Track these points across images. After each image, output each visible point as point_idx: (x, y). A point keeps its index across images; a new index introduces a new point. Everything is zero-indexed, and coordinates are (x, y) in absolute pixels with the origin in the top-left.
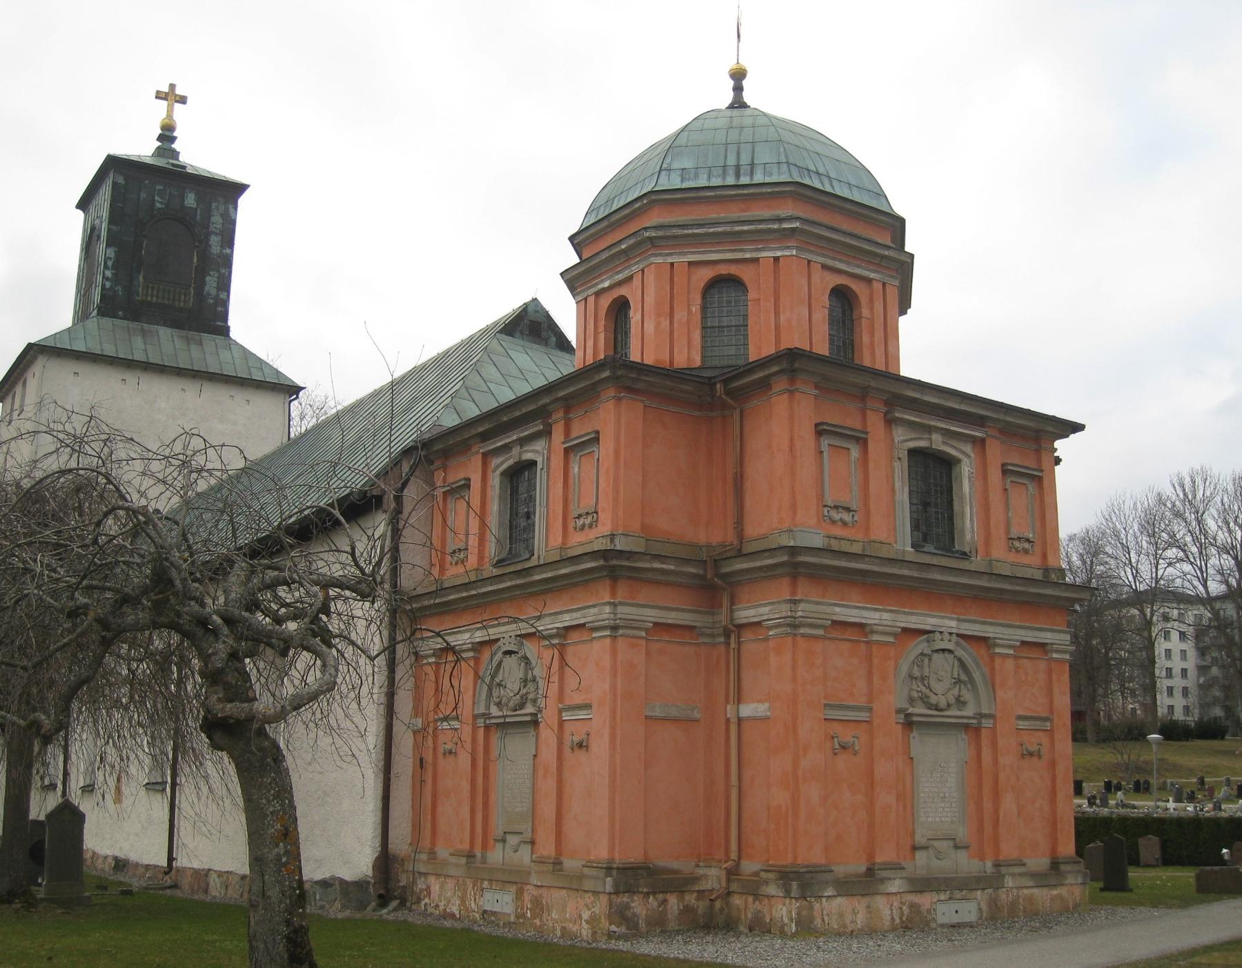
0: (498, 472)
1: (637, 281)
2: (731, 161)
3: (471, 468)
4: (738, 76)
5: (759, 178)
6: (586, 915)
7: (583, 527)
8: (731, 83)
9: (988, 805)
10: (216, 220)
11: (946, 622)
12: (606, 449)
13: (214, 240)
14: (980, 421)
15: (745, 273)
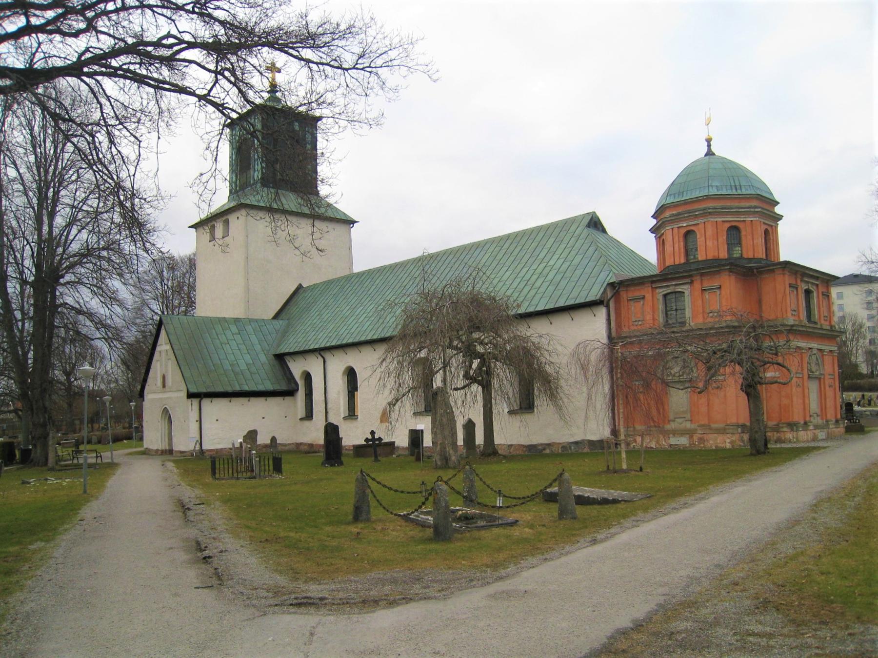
0: (661, 294)
1: (701, 226)
2: (733, 184)
3: (646, 291)
4: (709, 141)
5: (744, 191)
6: (728, 441)
7: (712, 317)
8: (706, 143)
9: (823, 401)
10: (309, 137)
11: (814, 345)
12: (725, 291)
13: (309, 146)
14: (817, 278)
15: (741, 226)
